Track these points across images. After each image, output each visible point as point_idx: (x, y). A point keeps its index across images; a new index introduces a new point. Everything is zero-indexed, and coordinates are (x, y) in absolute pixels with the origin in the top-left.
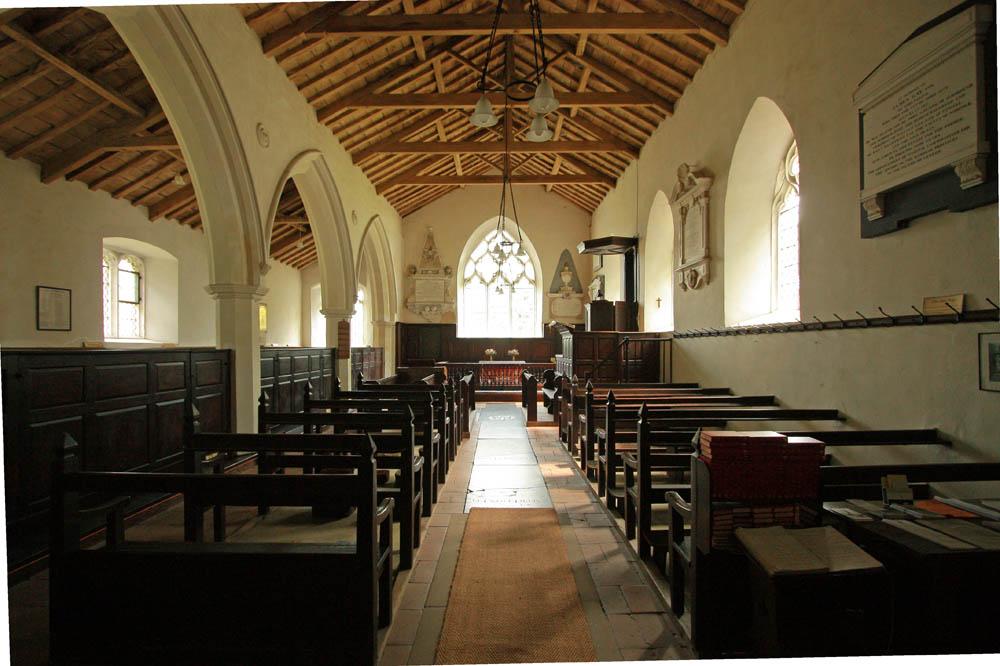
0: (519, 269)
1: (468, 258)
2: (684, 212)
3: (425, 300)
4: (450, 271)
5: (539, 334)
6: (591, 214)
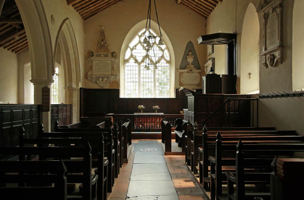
0: (160, 54)
1: (127, 47)
2: (266, 17)
3: (99, 73)
4: (115, 55)
5: (173, 96)
6: (206, 18)
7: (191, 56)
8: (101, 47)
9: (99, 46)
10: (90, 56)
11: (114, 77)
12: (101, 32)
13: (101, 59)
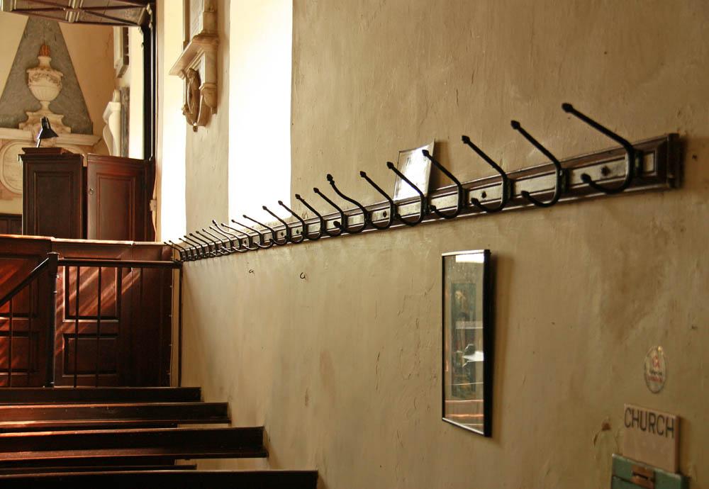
7: (45, 71)
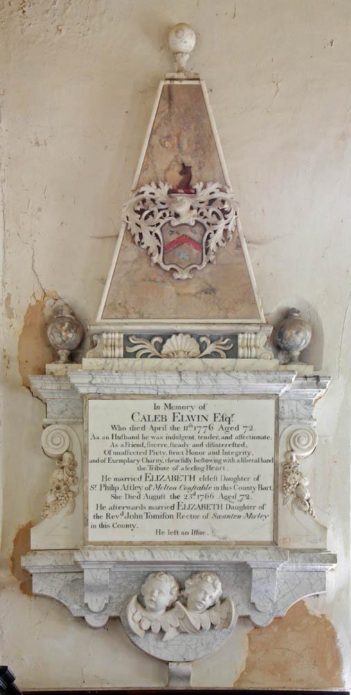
3: (146, 530)
8: (167, 249)
9: (149, 241)
10: (55, 358)
11: (293, 567)
12: (169, 94)
13: (170, 382)
